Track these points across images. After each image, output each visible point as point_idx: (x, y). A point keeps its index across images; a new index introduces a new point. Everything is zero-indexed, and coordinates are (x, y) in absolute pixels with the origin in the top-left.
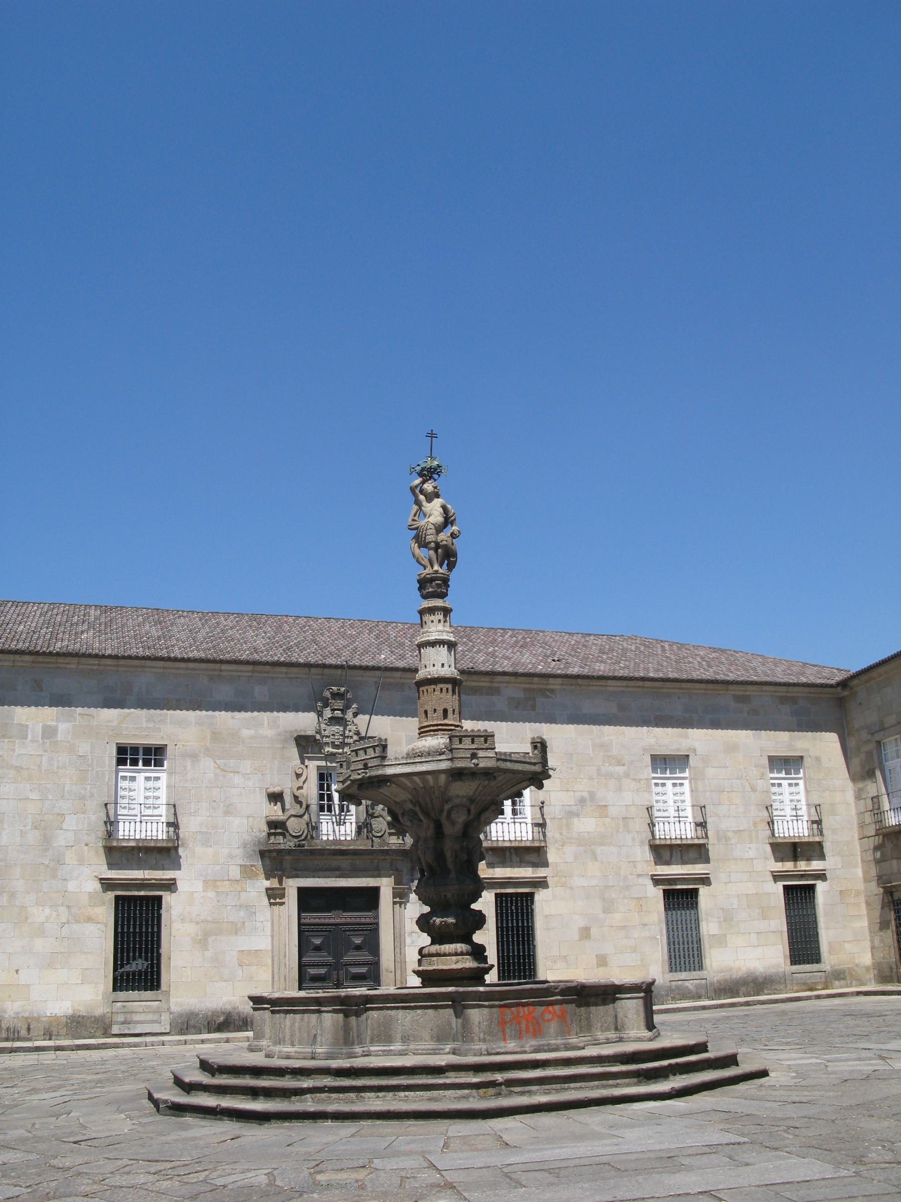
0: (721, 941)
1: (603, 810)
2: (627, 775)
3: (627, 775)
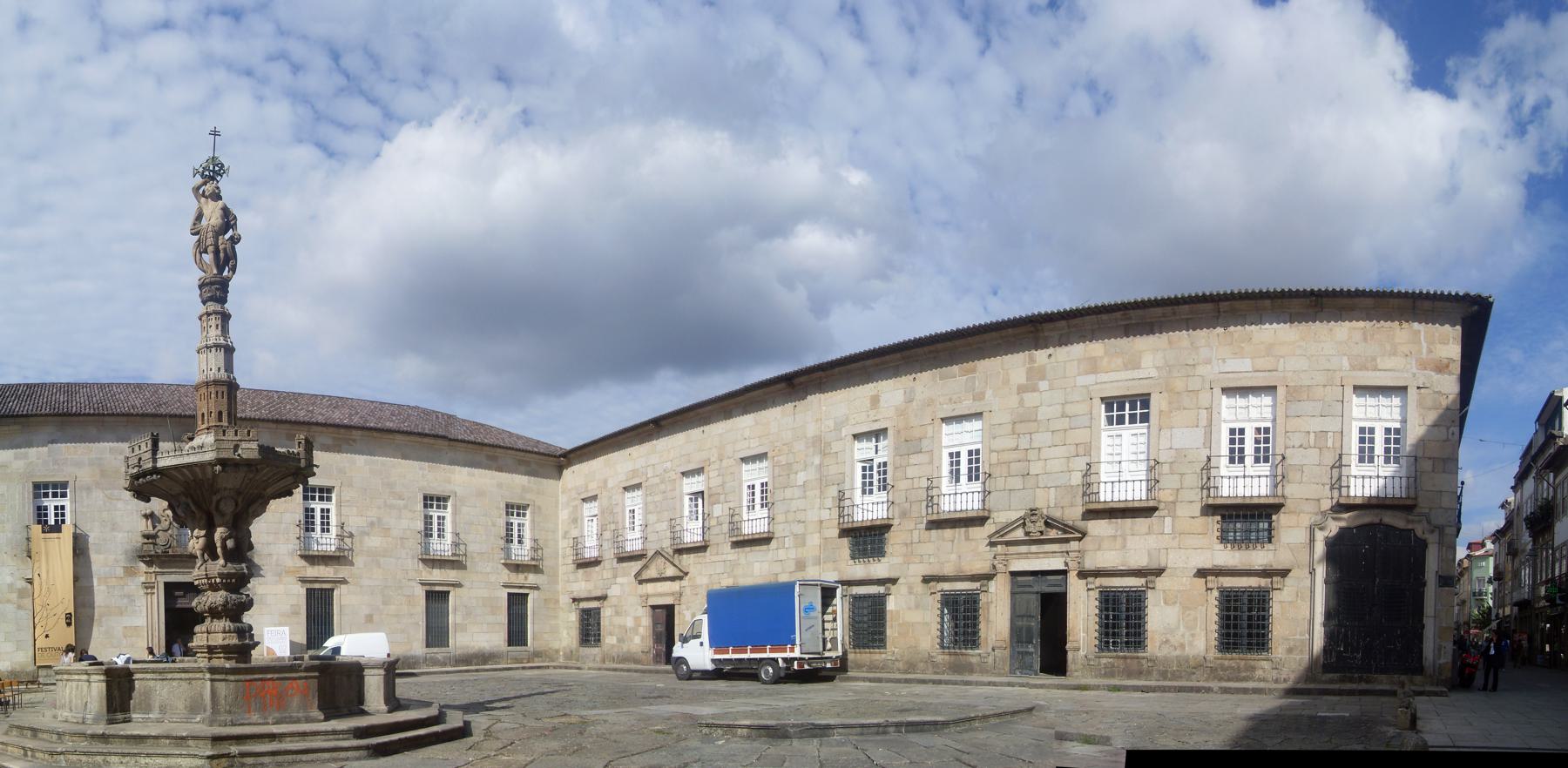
0: (463, 628)
2: (405, 507)
3: (405, 507)
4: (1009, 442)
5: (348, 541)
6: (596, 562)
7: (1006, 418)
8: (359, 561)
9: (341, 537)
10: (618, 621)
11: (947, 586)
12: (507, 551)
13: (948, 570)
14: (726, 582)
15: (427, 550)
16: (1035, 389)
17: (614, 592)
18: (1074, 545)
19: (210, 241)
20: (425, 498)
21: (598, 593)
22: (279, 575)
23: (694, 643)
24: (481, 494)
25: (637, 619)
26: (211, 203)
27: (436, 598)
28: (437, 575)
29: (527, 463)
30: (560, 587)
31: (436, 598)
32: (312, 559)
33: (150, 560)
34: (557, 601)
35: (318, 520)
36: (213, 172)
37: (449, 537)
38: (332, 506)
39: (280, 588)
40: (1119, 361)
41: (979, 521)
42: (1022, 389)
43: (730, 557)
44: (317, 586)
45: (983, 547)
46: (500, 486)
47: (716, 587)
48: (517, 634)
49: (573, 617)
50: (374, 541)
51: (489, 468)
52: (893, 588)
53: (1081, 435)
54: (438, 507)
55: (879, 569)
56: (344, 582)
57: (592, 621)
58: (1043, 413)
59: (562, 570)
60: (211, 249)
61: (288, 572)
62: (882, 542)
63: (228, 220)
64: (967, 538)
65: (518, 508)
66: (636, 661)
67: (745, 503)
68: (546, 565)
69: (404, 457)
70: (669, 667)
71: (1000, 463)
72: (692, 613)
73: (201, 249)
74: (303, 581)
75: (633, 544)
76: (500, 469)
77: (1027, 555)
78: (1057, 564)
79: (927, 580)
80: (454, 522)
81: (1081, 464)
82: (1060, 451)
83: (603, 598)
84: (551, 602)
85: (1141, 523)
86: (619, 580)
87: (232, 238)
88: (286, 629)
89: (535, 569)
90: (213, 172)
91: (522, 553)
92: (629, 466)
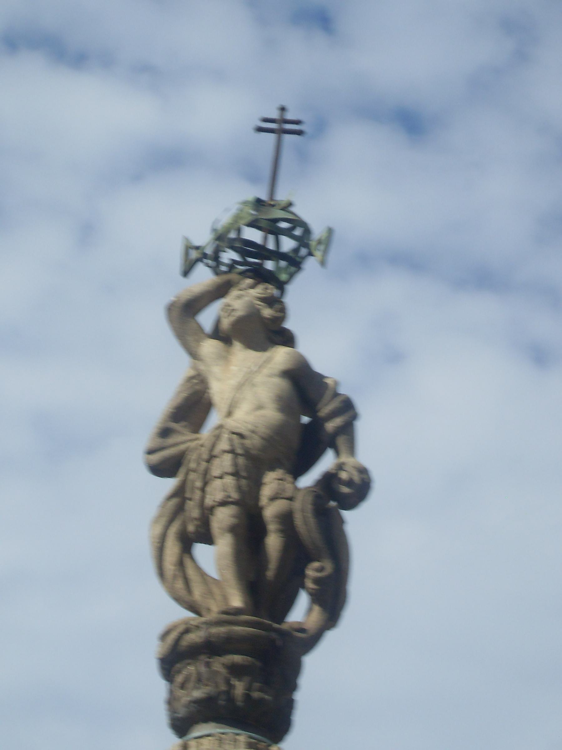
19: (222, 487)
26: (242, 357)
36: (261, 260)
60: (223, 517)
63: (313, 416)
73: (186, 529)
87: (329, 481)
90: (261, 260)
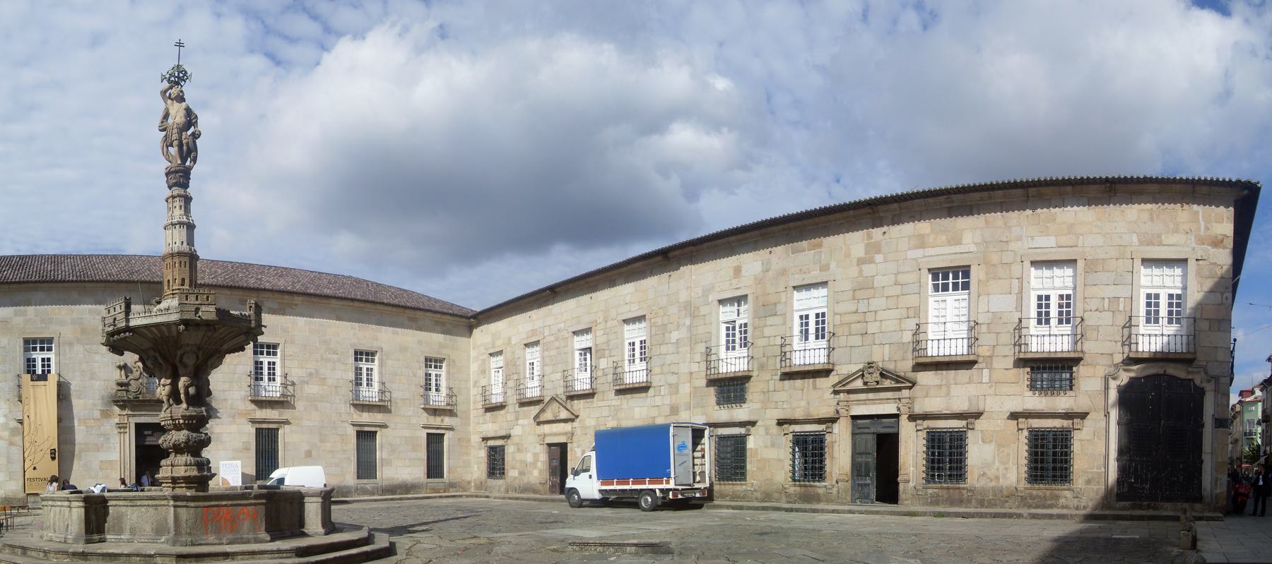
0: (387, 462)
1: (323, 380)
2: (339, 360)
3: (339, 360)
4: (851, 307)
5: (290, 388)
6: (501, 407)
7: (847, 286)
8: (300, 405)
9: (284, 385)
10: (519, 456)
11: (797, 428)
12: (426, 398)
13: (798, 415)
14: (611, 424)
15: (357, 396)
16: (871, 261)
17: (516, 432)
18: (905, 393)
19: (175, 136)
20: (356, 353)
21: (503, 433)
22: (233, 417)
23: (584, 476)
24: (403, 349)
25: (536, 455)
26: (176, 105)
27: (366, 437)
28: (366, 418)
29: (443, 324)
30: (471, 428)
31: (366, 437)
32: (261, 404)
33: (122, 404)
34: (469, 440)
35: (265, 371)
36: (178, 78)
37: (376, 386)
38: (277, 359)
39: (234, 428)
40: (944, 238)
41: (825, 372)
42: (861, 262)
43: (614, 403)
44: (265, 426)
45: (828, 395)
46: (420, 342)
47: (603, 428)
48: (434, 467)
49: (483, 454)
50: (312, 389)
51: (411, 328)
52: (753, 430)
53: (912, 300)
54: (367, 360)
55: (740, 413)
56: (287, 422)
57: (497, 457)
58: (879, 281)
59: (473, 414)
60: (175, 143)
61: (241, 414)
62: (743, 391)
63: (190, 119)
64: (815, 388)
65: (436, 361)
66: (535, 491)
67: (627, 357)
68: (460, 409)
69: (339, 319)
70: (563, 497)
71: (842, 324)
72: (582, 451)
73: (167, 143)
74: (253, 421)
75: (533, 392)
76: (420, 329)
77: (865, 402)
78: (890, 409)
79: (781, 423)
80: (381, 373)
81: (911, 324)
82: (894, 314)
83: (507, 437)
84: (464, 441)
85: (963, 374)
86: (521, 422)
87: (193, 134)
88: (239, 463)
89: (450, 413)
90: (178, 78)
91: (439, 399)
92: (529, 327)
